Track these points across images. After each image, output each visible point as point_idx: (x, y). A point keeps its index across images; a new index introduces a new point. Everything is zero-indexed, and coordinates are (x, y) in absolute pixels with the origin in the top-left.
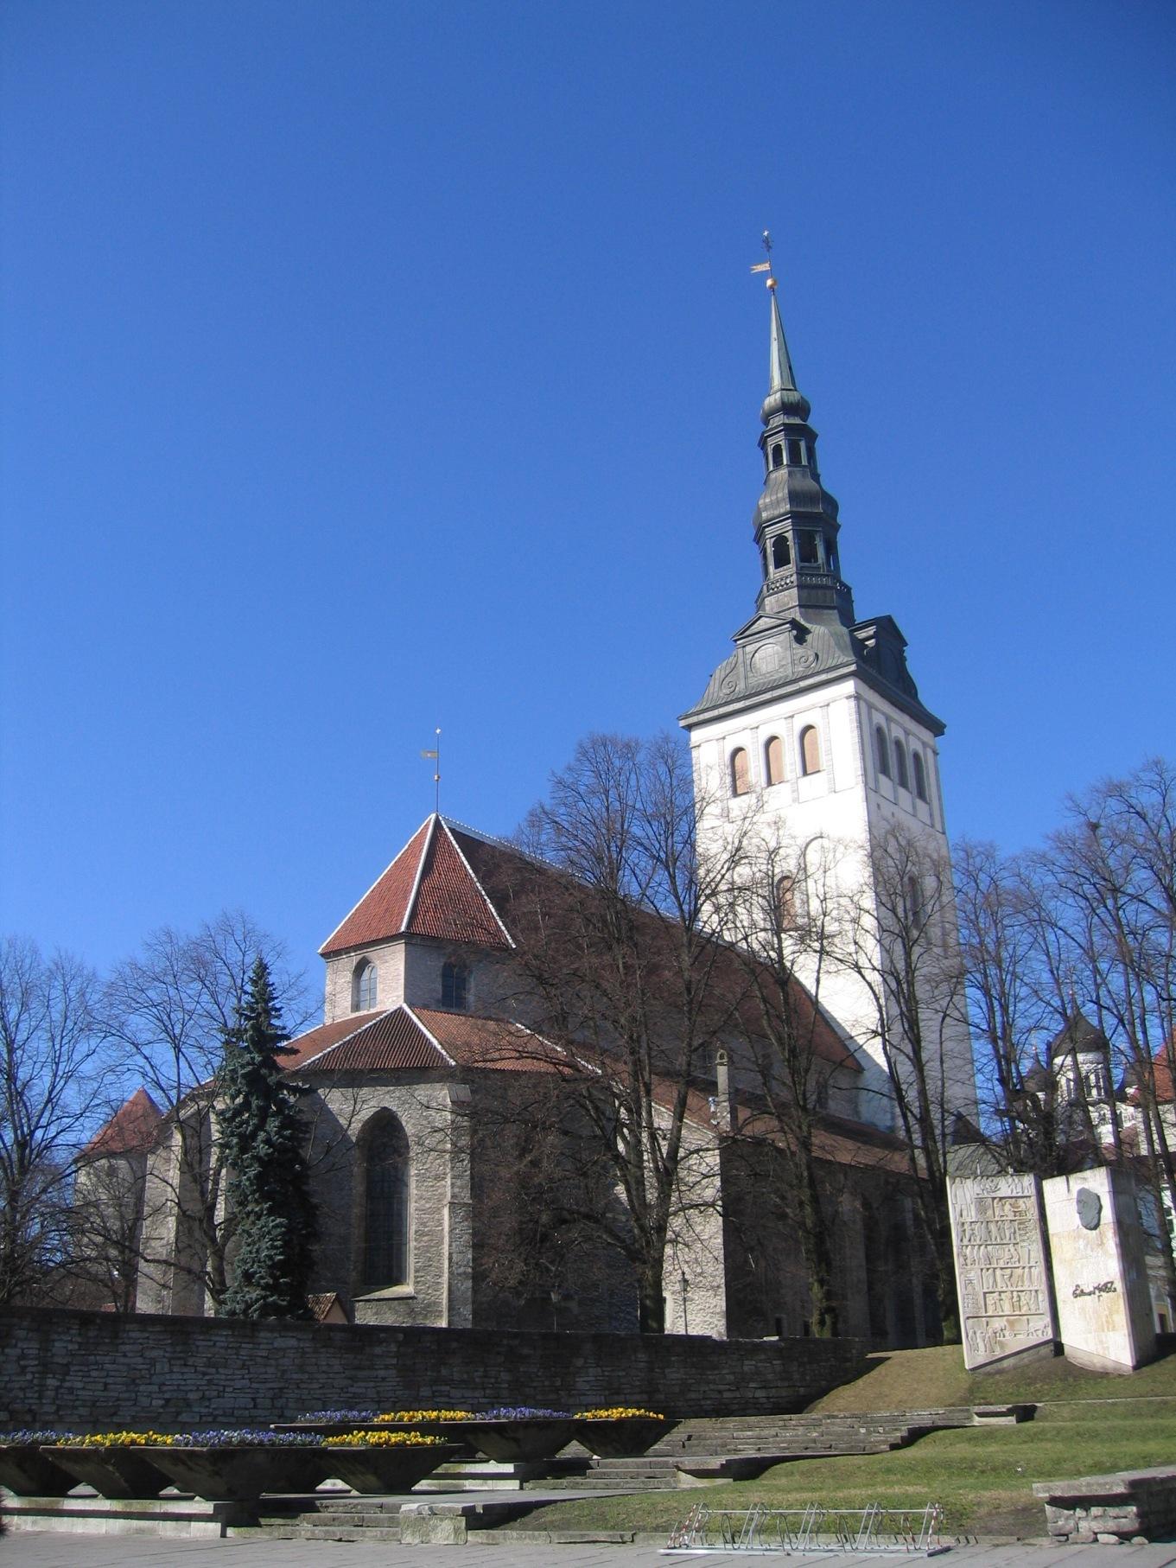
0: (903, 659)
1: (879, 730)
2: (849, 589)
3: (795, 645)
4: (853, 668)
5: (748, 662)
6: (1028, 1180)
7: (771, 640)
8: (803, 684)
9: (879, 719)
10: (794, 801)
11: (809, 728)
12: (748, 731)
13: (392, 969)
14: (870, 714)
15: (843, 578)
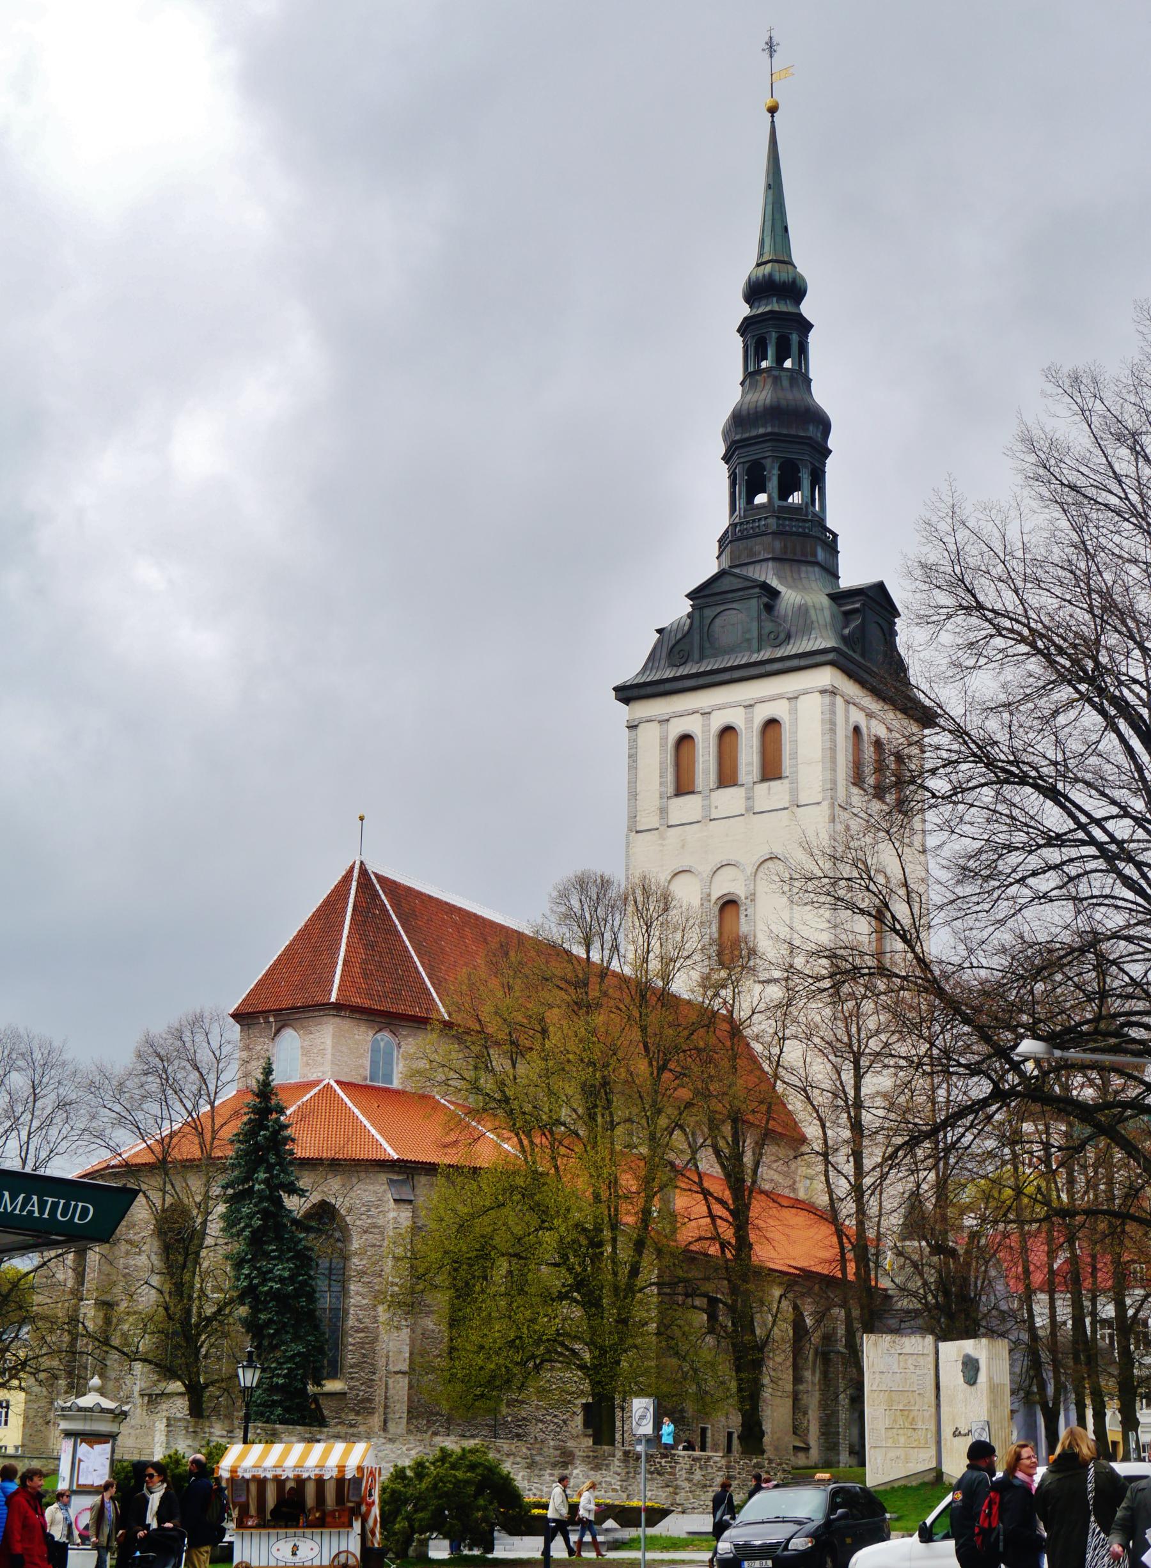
0: (894, 634)
1: (857, 730)
2: (835, 536)
3: (764, 615)
4: (831, 656)
5: (706, 629)
6: (930, 1339)
7: (734, 605)
8: (769, 668)
9: (857, 717)
10: (747, 810)
11: (772, 724)
12: (698, 715)
13: (318, 1041)
14: (847, 711)
15: (829, 525)
